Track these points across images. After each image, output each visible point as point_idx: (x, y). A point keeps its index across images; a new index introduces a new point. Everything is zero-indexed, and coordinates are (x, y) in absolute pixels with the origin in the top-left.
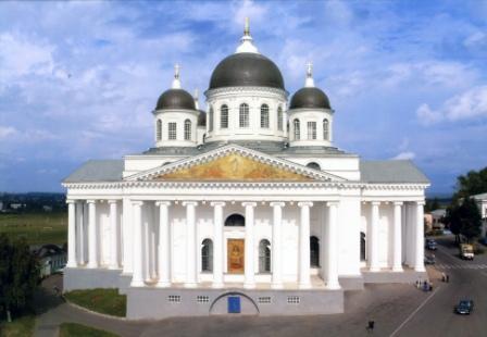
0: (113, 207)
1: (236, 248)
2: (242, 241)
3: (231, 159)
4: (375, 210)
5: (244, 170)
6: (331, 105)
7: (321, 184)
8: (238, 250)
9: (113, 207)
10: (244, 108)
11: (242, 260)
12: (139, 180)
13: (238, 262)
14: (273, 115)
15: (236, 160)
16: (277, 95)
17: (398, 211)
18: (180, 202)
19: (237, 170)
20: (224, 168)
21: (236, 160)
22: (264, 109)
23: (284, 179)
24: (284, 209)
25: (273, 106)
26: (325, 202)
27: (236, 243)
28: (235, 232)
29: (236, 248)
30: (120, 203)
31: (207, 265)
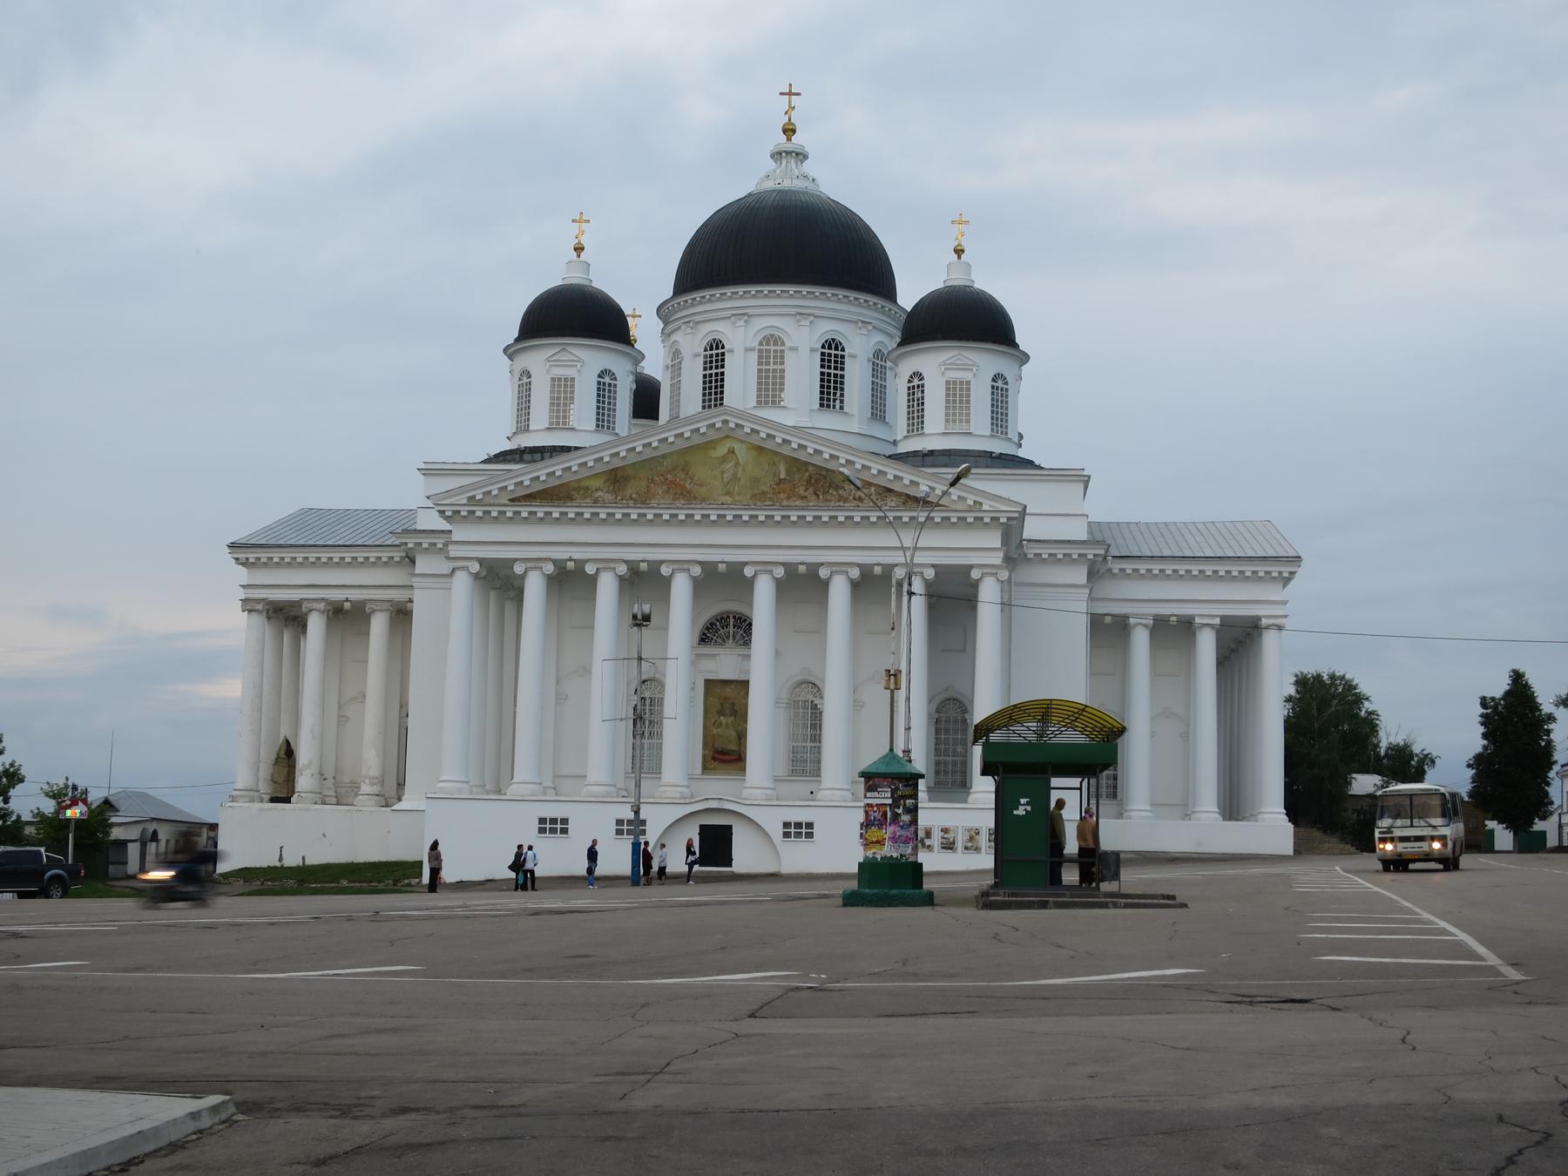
0: (379, 624)
2: (744, 685)
3: (722, 450)
4: (1141, 640)
5: (755, 481)
6: (1019, 339)
8: (734, 713)
9: (379, 624)
10: (771, 352)
13: (734, 748)
14: (856, 377)
15: (731, 451)
16: (868, 314)
17: (1206, 646)
18: (581, 564)
19: (735, 478)
20: (700, 472)
21: (731, 451)
22: (832, 357)
24: (856, 586)
25: (860, 347)
26: (971, 567)
28: (724, 665)
30: (401, 615)
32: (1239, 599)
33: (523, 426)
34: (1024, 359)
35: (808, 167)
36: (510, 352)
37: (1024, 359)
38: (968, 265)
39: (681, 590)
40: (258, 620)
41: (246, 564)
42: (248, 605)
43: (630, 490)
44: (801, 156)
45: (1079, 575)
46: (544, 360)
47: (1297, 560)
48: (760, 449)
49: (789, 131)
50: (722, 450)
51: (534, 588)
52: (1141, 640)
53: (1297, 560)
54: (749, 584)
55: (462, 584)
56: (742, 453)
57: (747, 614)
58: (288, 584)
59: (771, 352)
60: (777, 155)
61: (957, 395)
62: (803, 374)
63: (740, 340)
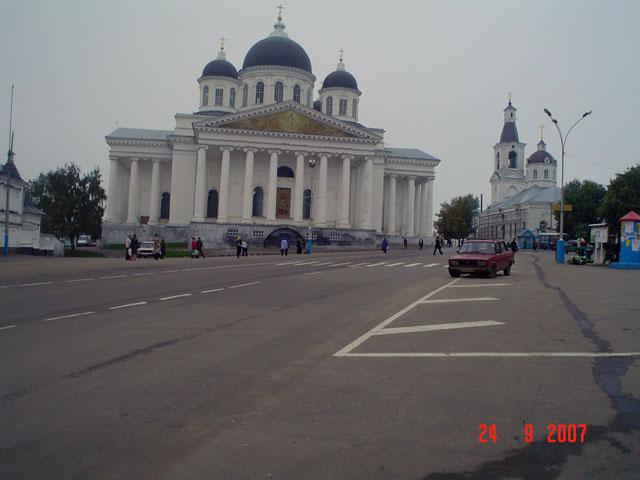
1: (284, 195)
4: (393, 182)
7: (361, 140)
10: (279, 87)
11: (288, 206)
12: (207, 125)
18: (242, 148)
20: (281, 121)
23: (331, 134)
25: (304, 87)
26: (364, 157)
27: (283, 192)
28: (285, 182)
29: (284, 195)
30: (166, 165)
31: (257, 210)
32: (421, 171)
33: (205, 102)
34: (360, 94)
35: (285, 30)
36: (199, 81)
37: (360, 94)
38: (343, 65)
39: (274, 158)
40: (115, 163)
41: (110, 145)
42: (112, 158)
43: (259, 125)
44: (283, 27)
45: (383, 161)
46: (213, 84)
47: (439, 161)
48: (302, 115)
49: (280, 19)
50: (288, 115)
51: (226, 156)
52: (393, 182)
53: (439, 161)
54: (296, 158)
55: (202, 154)
56: (294, 116)
57: (292, 168)
58: (125, 151)
59: (279, 87)
60: (276, 26)
61: (343, 104)
62: (288, 95)
63: (270, 84)
